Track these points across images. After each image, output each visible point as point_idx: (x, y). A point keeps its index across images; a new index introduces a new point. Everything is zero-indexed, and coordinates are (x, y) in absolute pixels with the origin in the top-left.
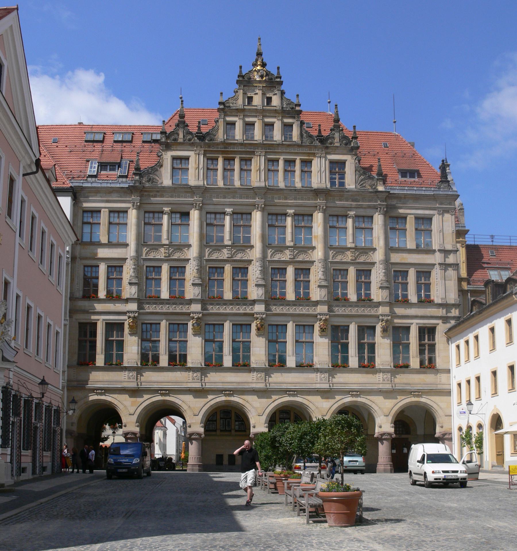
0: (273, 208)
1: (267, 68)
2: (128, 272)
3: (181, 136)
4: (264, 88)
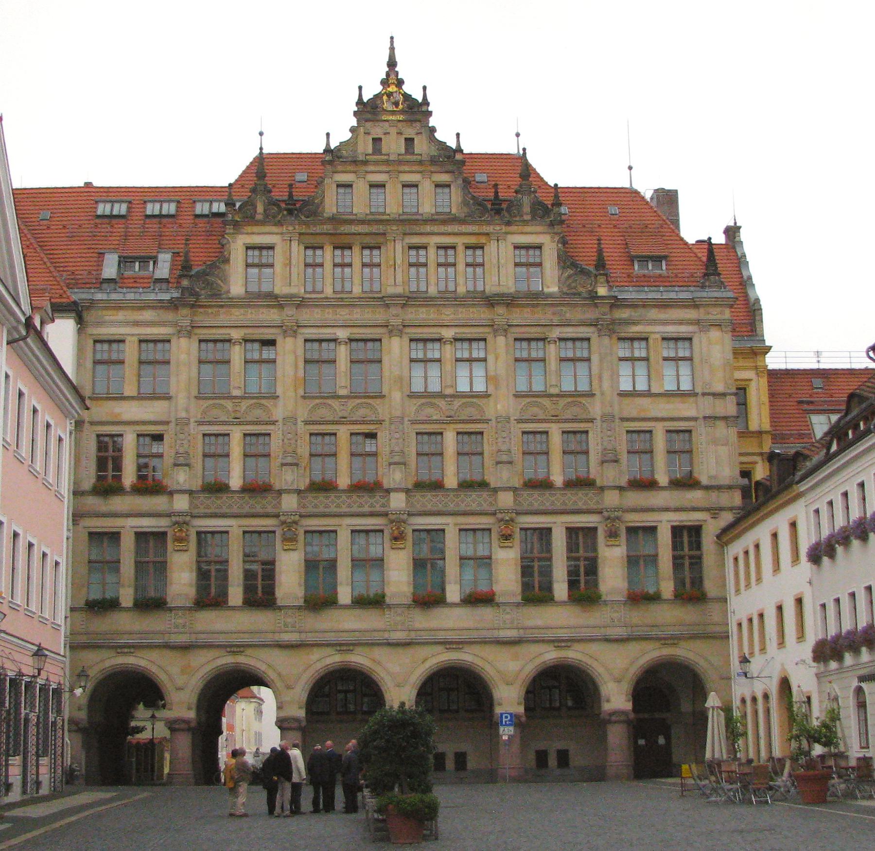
0: (419, 330)
1: (406, 88)
3: (260, 208)
4: (400, 125)
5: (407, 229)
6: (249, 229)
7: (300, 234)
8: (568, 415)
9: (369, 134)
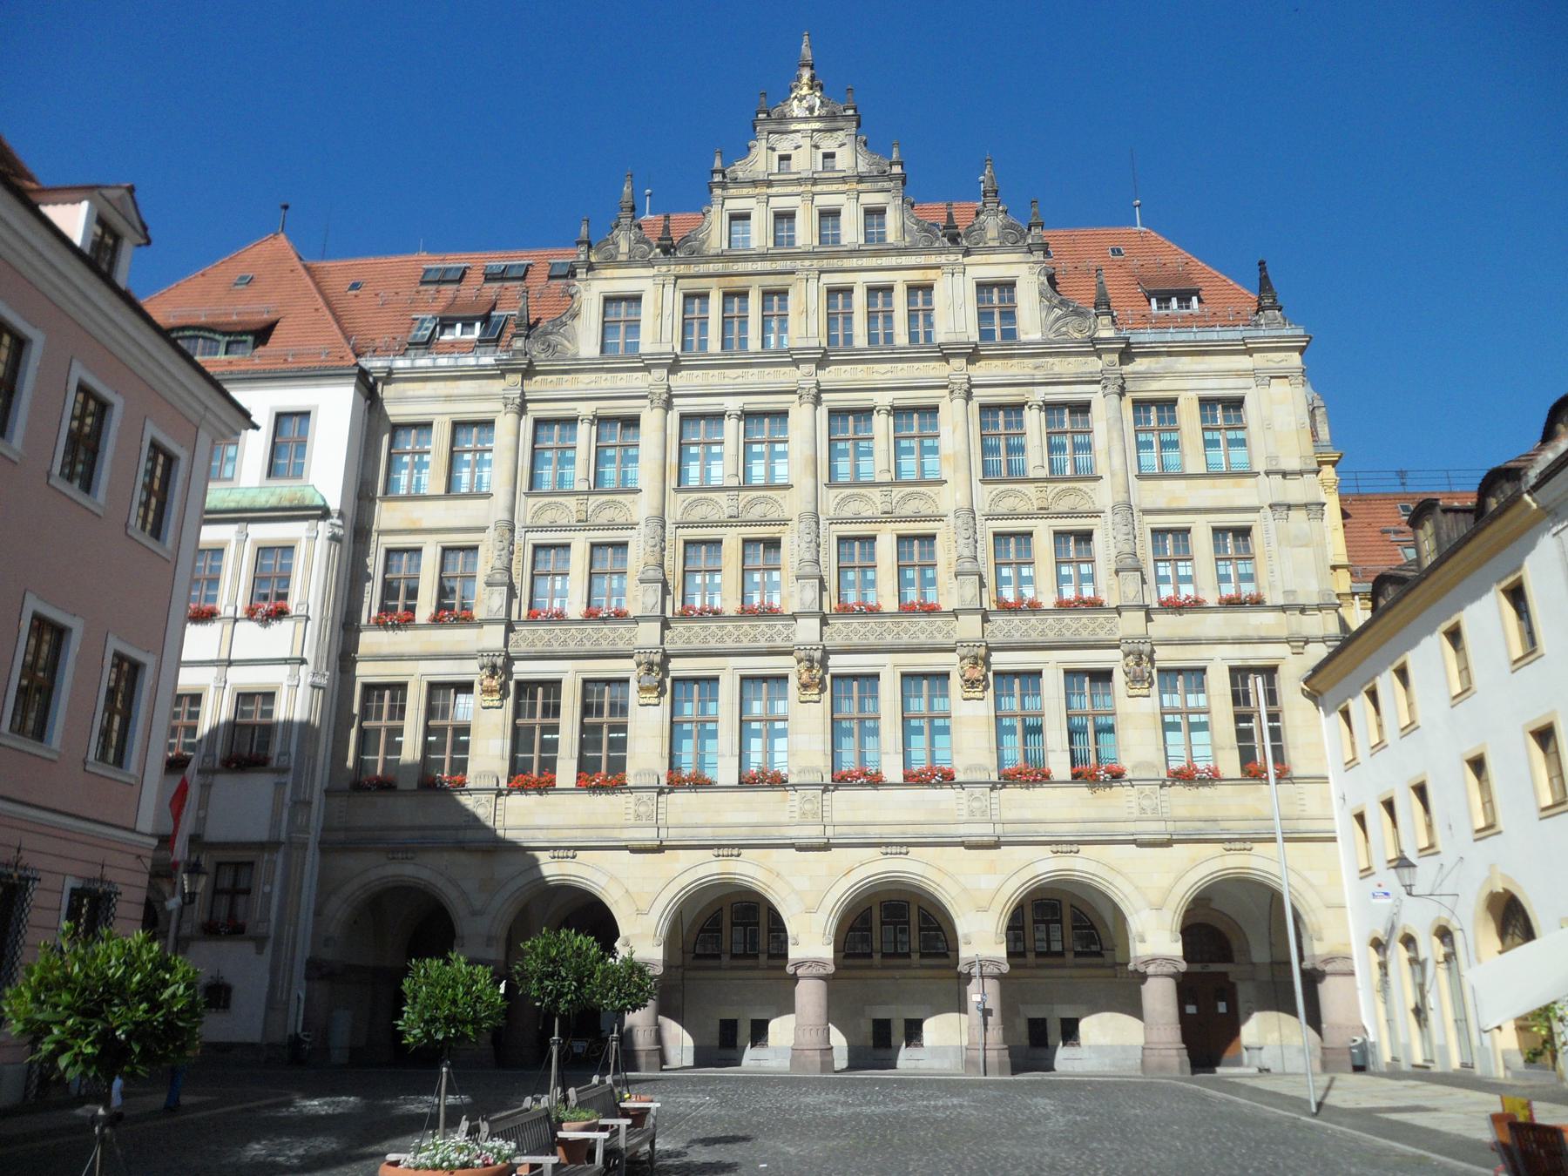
2: (487, 561)
3: (624, 247)
5: (825, 264)
6: (608, 273)
7: (677, 277)
8: (1064, 506)
9: (774, 150)
